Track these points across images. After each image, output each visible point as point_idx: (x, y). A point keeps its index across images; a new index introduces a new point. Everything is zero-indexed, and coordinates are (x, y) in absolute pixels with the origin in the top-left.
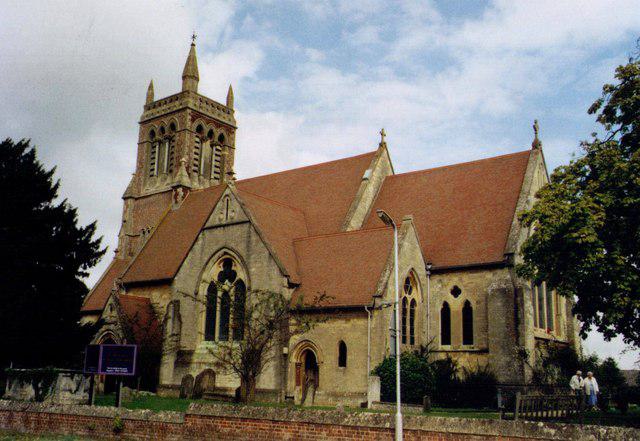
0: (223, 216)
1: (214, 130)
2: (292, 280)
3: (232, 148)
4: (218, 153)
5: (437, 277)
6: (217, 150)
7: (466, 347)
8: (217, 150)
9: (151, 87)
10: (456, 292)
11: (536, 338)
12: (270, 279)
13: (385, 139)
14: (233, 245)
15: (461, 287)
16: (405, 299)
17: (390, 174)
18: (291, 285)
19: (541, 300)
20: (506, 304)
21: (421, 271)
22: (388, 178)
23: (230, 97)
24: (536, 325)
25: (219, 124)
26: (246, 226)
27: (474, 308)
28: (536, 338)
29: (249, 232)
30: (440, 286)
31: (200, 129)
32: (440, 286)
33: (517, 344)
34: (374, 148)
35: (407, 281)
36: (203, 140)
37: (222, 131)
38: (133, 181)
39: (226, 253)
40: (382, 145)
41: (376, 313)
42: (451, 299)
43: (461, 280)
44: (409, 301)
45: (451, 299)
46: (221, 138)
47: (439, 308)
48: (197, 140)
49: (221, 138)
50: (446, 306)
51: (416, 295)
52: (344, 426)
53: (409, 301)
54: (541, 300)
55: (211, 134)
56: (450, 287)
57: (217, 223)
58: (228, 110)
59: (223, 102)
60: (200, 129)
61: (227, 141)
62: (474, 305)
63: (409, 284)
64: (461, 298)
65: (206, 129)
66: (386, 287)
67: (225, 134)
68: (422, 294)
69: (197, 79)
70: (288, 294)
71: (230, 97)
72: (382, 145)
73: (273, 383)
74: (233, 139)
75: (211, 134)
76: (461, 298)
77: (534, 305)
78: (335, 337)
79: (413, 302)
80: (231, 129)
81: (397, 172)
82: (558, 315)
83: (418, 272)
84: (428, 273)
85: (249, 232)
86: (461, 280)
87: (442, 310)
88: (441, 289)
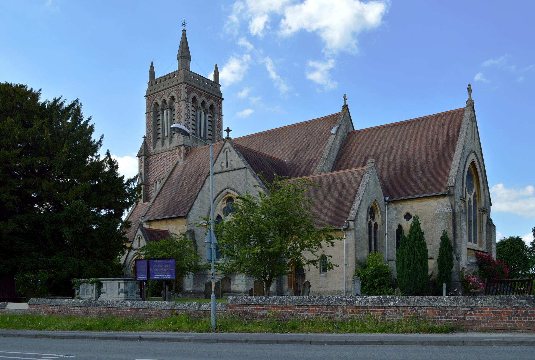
0: (224, 164)
1: (206, 101)
4: (210, 119)
5: (393, 206)
6: (209, 117)
8: (209, 117)
14: (233, 186)
21: (381, 201)
28: (468, 249)
29: (246, 176)
30: (395, 212)
31: (194, 100)
32: (395, 212)
34: (339, 109)
37: (212, 101)
38: (145, 143)
39: (228, 193)
40: (345, 107)
44: (373, 223)
46: (212, 107)
47: (396, 228)
49: (212, 107)
50: (400, 226)
51: (378, 219)
52: (357, 307)
53: (373, 223)
55: (203, 103)
56: (404, 213)
63: (372, 212)
65: (200, 100)
66: (357, 214)
72: (345, 107)
74: (221, 108)
75: (203, 103)
79: (376, 224)
84: (386, 203)
87: (397, 230)
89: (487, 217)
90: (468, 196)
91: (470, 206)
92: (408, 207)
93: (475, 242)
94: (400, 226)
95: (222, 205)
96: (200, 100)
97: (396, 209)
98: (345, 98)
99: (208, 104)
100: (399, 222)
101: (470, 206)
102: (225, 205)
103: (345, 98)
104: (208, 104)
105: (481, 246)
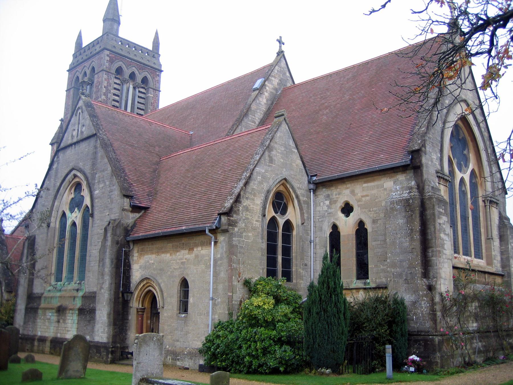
1: (137, 72)
2: (137, 203)
3: (157, 90)
5: (323, 192)
6: (139, 92)
7: (360, 284)
8: (139, 92)
9: (80, 37)
10: (347, 209)
11: (454, 268)
12: (112, 202)
13: (284, 48)
14: (81, 165)
15: (353, 202)
16: (273, 222)
17: (289, 84)
18: (135, 209)
19: (464, 218)
20: (409, 220)
22: (286, 90)
23: (156, 43)
24: (456, 251)
25: (143, 66)
26: (92, 141)
27: (369, 230)
28: (454, 268)
30: (327, 202)
31: (119, 71)
32: (327, 202)
33: (426, 274)
34: (270, 58)
35: (279, 196)
36: (123, 82)
40: (281, 54)
41: (221, 238)
42: (341, 220)
43: (353, 193)
44: (281, 221)
45: (341, 220)
46: (145, 80)
47: (328, 231)
48: (118, 81)
49: (145, 80)
54: (464, 218)
55: (132, 76)
56: (340, 204)
57: (70, 142)
58: (155, 52)
59: (150, 47)
60: (119, 71)
61: (151, 84)
62: (368, 226)
64: (354, 218)
65: (127, 72)
66: (238, 200)
67: (149, 77)
68: (302, 214)
69: (119, 23)
70: (131, 218)
71: (156, 43)
72: (281, 54)
73: (106, 335)
74: (159, 82)
75: (132, 76)
76: (354, 218)
77: (453, 224)
78: (177, 273)
79: (288, 225)
80: (157, 71)
81: (297, 82)
82: (489, 239)
83: (296, 185)
84: (312, 186)
85: (96, 147)
86: (353, 193)
87: (331, 234)
88: (329, 207)
89: (500, 213)
90: (459, 175)
91: (463, 193)
92: (347, 192)
93: (478, 255)
94: (335, 227)
95: (68, 196)
96: (127, 72)
97: (328, 196)
98: (280, 42)
99: (139, 78)
100: (332, 220)
101: (463, 193)
102: (73, 196)
103: (280, 42)
104: (139, 78)
105: (489, 263)
